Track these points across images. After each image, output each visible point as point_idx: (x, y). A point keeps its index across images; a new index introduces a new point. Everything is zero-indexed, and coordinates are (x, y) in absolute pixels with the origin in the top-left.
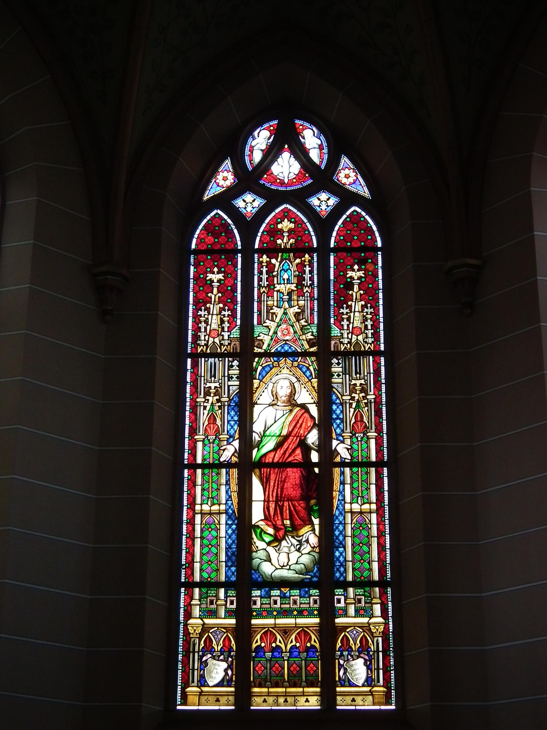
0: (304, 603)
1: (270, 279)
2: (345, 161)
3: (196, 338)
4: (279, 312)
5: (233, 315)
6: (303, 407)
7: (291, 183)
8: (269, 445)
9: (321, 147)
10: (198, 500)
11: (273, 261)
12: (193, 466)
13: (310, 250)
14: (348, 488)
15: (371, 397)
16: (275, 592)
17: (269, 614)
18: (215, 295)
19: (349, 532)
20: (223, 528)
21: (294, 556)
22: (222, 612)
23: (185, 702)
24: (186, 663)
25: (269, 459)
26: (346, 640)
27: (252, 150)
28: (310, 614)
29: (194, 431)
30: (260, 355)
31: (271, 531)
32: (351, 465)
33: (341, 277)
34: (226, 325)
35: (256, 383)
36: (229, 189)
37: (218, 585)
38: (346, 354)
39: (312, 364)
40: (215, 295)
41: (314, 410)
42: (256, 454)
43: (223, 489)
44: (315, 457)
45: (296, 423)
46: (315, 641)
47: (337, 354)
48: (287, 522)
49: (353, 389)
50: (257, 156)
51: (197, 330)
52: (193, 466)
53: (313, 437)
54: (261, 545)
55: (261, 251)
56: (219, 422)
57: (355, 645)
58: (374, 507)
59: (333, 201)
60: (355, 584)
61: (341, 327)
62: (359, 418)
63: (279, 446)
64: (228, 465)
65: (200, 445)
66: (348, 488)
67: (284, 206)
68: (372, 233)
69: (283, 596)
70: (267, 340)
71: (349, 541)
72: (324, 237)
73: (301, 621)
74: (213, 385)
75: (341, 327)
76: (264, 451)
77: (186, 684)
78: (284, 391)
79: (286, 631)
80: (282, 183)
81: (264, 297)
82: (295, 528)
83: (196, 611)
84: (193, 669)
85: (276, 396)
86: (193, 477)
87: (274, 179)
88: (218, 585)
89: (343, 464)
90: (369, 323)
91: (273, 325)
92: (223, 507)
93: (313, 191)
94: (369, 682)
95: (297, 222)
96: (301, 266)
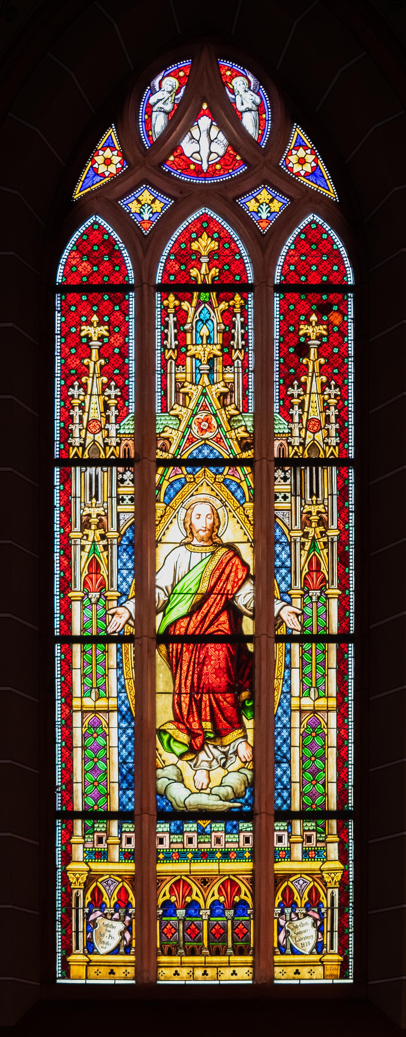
1: (180, 336)
3: (66, 433)
4: (195, 391)
5: (124, 397)
6: (231, 547)
7: (211, 172)
9: (260, 109)
10: (77, 690)
11: (185, 305)
14: (296, 674)
15: (333, 533)
16: (190, 827)
17: (182, 856)
19: (296, 739)
20: (114, 733)
21: (217, 774)
22: (115, 853)
23: (67, 975)
24: (66, 924)
25: (180, 630)
26: (288, 893)
27: (149, 109)
28: (240, 856)
29: (66, 585)
30: (165, 463)
31: (184, 738)
32: (302, 639)
34: (113, 412)
35: (160, 507)
36: (116, 180)
37: (108, 816)
43: (113, 674)
44: (248, 627)
46: (245, 895)
47: (282, 462)
48: (207, 725)
49: (306, 523)
54: (171, 758)
55: (165, 289)
56: (104, 571)
57: (301, 900)
58: (333, 702)
60: (303, 815)
61: (289, 418)
63: (196, 608)
64: (121, 639)
65: (76, 607)
66: (296, 674)
67: (203, 210)
68: (341, 263)
69: (202, 832)
70: (176, 436)
71: (296, 754)
73: (227, 866)
74: (94, 512)
75: (289, 418)
76: (172, 616)
77: (68, 951)
79: (205, 882)
80: (198, 171)
81: (171, 366)
82: (219, 734)
83: (78, 852)
84: (77, 932)
86: (68, 654)
88: (108, 816)
89: (289, 638)
90: (333, 412)
91: (185, 413)
92: (113, 703)
94: (319, 947)
95: (223, 239)
96: (228, 315)
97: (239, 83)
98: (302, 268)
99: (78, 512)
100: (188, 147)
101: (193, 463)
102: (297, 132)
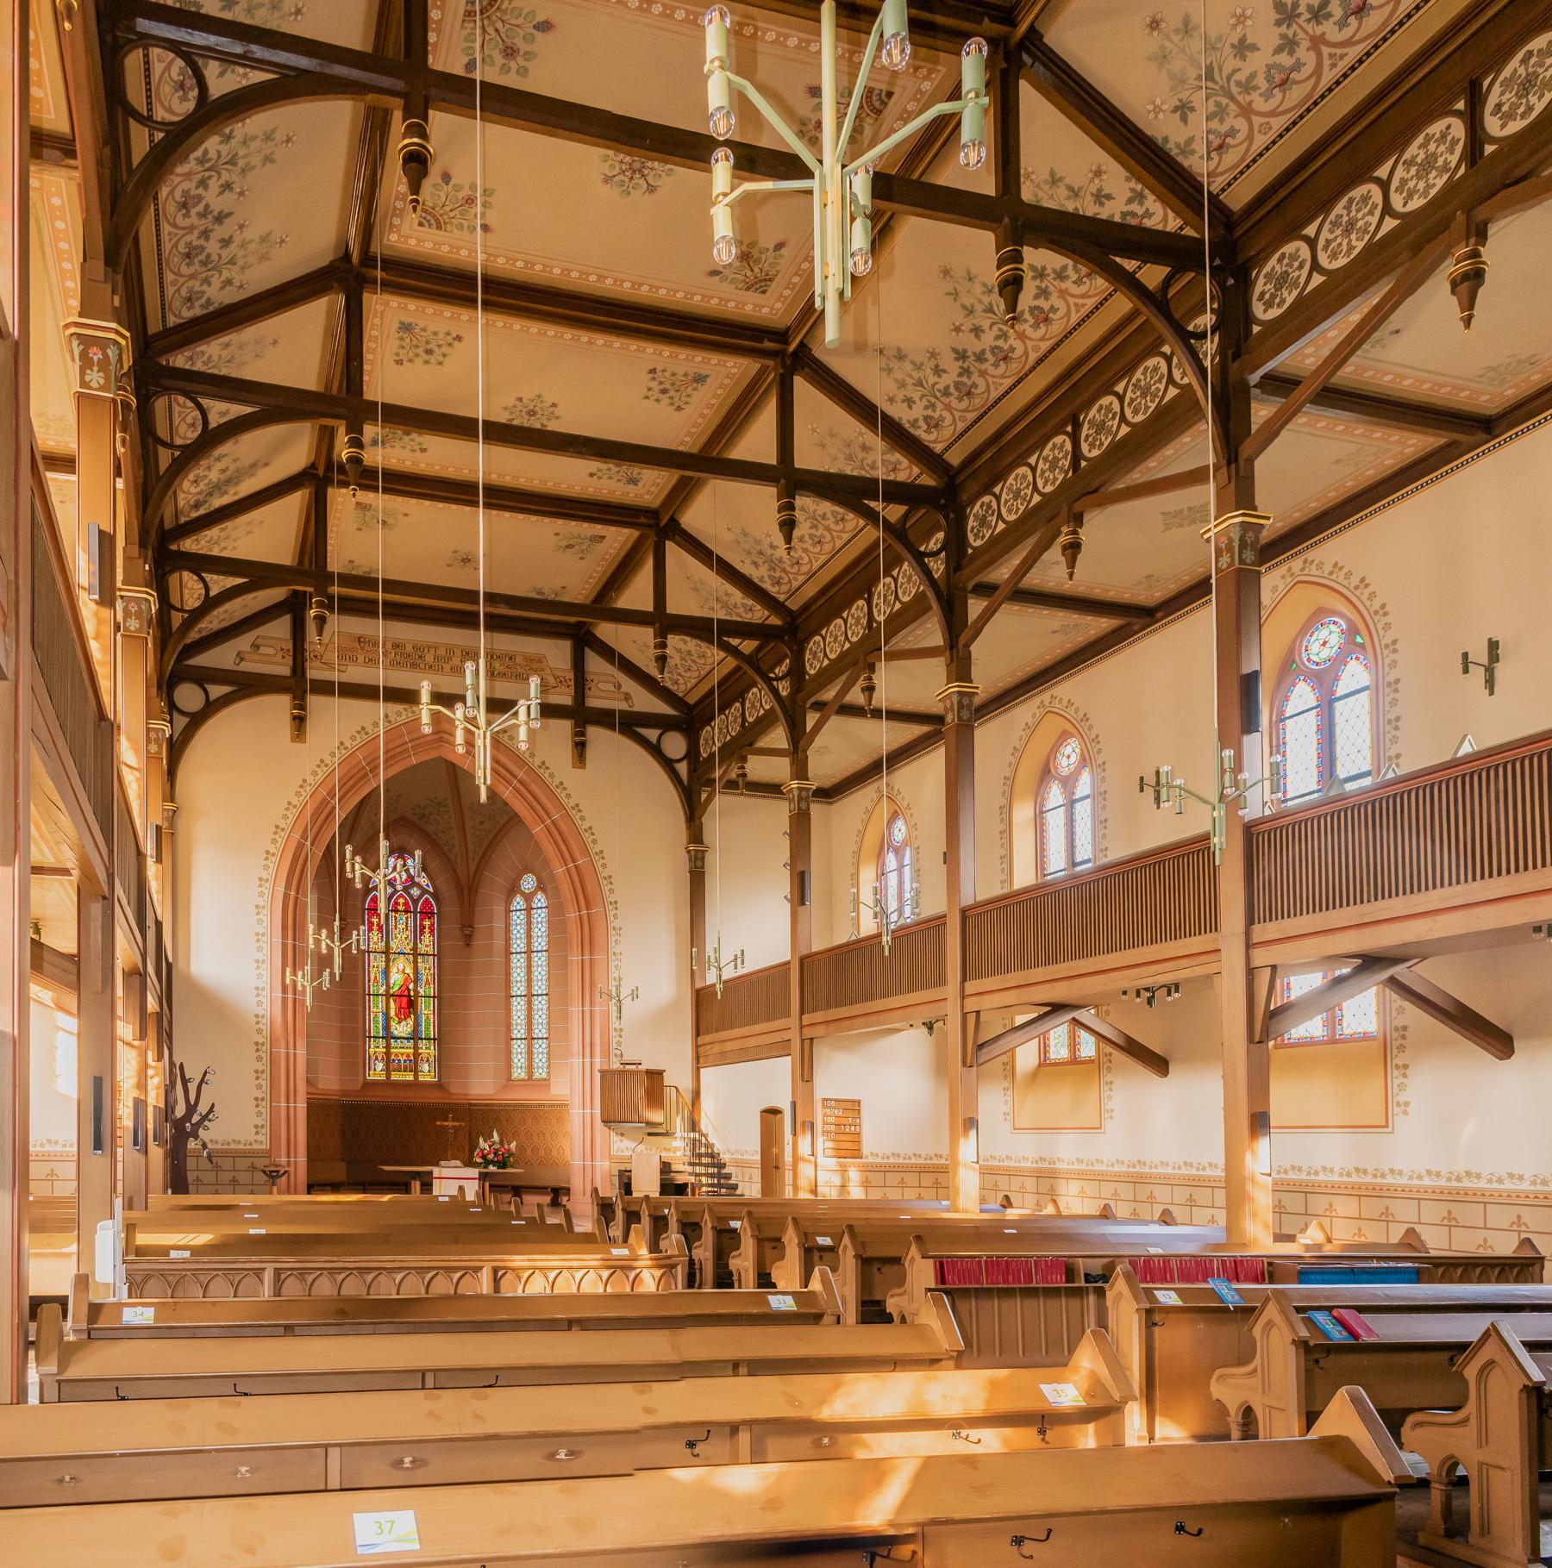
0: (408, 1045)
8: (396, 988)
33: (421, 925)
39: (411, 957)
42: (391, 991)
45: (406, 980)
78: (401, 968)
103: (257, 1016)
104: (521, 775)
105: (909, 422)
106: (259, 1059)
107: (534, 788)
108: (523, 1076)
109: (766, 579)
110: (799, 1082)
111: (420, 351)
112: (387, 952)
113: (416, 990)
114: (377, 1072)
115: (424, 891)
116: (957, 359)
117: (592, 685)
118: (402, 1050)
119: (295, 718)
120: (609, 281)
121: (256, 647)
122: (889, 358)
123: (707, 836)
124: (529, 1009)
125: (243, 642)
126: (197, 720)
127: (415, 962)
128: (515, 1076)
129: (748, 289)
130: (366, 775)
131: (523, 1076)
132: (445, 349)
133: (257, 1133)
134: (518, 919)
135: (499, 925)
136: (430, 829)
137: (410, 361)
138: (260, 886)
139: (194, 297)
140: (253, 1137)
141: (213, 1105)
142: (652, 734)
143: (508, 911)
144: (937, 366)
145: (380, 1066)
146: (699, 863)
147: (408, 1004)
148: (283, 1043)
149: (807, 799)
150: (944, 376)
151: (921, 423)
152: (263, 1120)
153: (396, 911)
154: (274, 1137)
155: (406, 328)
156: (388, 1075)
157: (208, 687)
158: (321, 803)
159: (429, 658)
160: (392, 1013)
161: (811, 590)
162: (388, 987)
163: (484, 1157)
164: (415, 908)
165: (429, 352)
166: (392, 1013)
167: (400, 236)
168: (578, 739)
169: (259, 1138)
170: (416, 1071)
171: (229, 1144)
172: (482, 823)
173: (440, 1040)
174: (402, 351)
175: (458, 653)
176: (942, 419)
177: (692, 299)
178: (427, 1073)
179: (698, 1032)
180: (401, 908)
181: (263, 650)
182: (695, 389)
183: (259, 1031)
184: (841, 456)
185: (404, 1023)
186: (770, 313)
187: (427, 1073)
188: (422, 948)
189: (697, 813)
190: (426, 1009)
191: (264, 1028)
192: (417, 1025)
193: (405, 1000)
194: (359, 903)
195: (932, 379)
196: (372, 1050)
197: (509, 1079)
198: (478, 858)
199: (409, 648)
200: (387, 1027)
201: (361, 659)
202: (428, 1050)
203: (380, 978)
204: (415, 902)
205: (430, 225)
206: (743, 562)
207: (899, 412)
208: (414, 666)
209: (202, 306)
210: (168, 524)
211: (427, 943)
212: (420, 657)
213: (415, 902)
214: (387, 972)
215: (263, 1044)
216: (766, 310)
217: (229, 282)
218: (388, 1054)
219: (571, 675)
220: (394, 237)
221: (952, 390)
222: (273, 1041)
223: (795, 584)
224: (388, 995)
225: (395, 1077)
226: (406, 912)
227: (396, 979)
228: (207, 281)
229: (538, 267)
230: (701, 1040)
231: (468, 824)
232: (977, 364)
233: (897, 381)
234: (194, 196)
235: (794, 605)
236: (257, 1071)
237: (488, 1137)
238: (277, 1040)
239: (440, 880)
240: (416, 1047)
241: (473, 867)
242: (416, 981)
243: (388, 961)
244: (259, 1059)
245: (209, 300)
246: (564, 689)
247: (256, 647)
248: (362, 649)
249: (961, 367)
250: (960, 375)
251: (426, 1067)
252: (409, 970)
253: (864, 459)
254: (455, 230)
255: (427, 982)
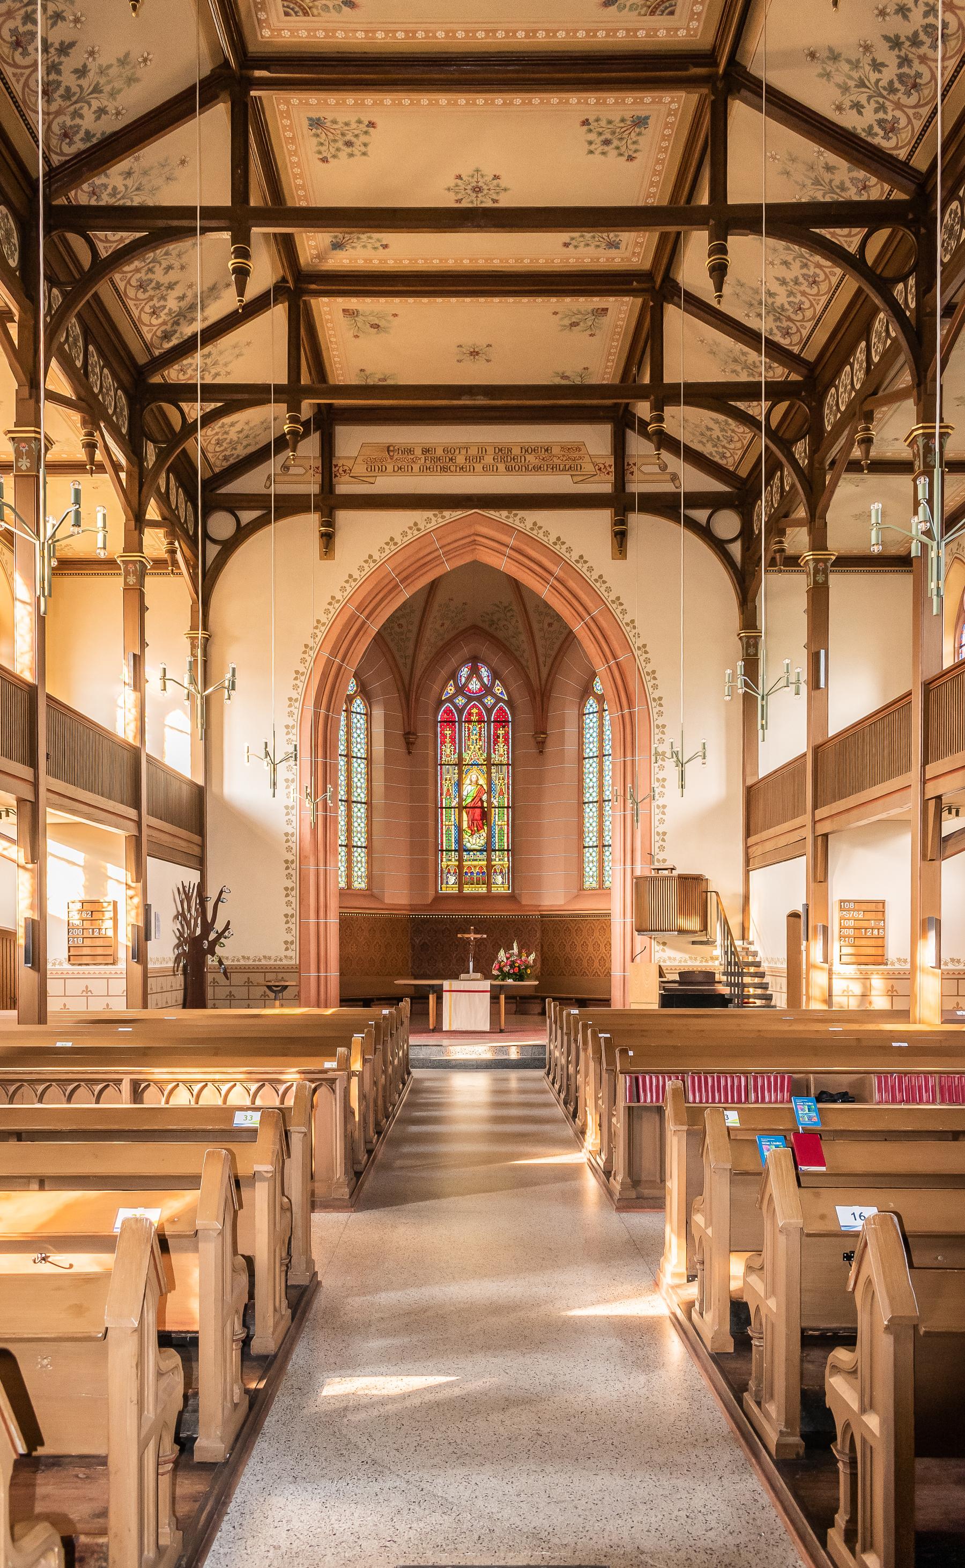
0: (481, 857)
2: (497, 682)
8: (469, 800)
12: (442, 808)
13: (484, 722)
18: (448, 740)
29: (441, 794)
33: (495, 734)
36: (453, 695)
38: (497, 765)
40: (448, 740)
41: (485, 787)
42: (464, 804)
44: (485, 804)
45: (479, 792)
46: (485, 870)
47: (493, 765)
50: (463, 680)
51: (441, 754)
52: (442, 808)
53: (485, 797)
55: (465, 722)
57: (498, 871)
59: (492, 701)
62: (501, 790)
68: (506, 714)
72: (489, 716)
73: (481, 863)
78: (474, 780)
79: (475, 867)
85: (471, 781)
87: (469, 690)
93: (485, 696)
94: (503, 883)
95: (479, 709)
96: (480, 728)
97: (483, 670)
98: (499, 717)
99: (444, 777)
100: (470, 686)
101: (472, 765)
102: (497, 682)
103: (286, 834)
104: (557, 571)
105: (864, 130)
106: (289, 876)
107: (571, 584)
108: (594, 885)
109: (775, 331)
110: (812, 885)
111: (340, 144)
112: (460, 764)
113: (489, 801)
114: (450, 885)
115: (499, 700)
116: (892, 48)
117: (635, 469)
118: (475, 863)
119: (323, 535)
120: (500, 34)
121: (286, 468)
122: (823, 62)
123: (762, 622)
124: (601, 815)
125: (272, 465)
126: (229, 547)
127: (489, 773)
128: (587, 885)
129: (653, 13)
130: (397, 586)
131: (594, 885)
132: (363, 138)
133: (287, 949)
134: (591, 722)
135: (570, 730)
136: (500, 635)
137: (334, 156)
138: (290, 706)
139: (70, 132)
140: (283, 954)
141: (229, 922)
142: (701, 515)
143: (582, 715)
144: (874, 60)
145: (452, 879)
146: (751, 651)
147: (482, 815)
148: (312, 860)
149: (825, 572)
150: (884, 70)
151: (877, 129)
152: (293, 936)
153: (470, 722)
154: (303, 953)
155: (316, 123)
156: (461, 888)
157: (238, 513)
158: (350, 620)
159: (460, 459)
160: (465, 825)
161: (821, 337)
162: (461, 799)
163: (500, 969)
164: (489, 717)
165: (349, 144)
166: (465, 825)
167: (272, 30)
168: (617, 528)
169: (289, 953)
170: (489, 884)
171: (260, 960)
172: (550, 625)
173: (513, 851)
174: (323, 149)
175: (490, 451)
176: (896, 120)
177: (595, 36)
178: (500, 885)
179: (748, 833)
180: (474, 718)
181: (293, 471)
182: (639, 134)
183: (289, 849)
184: (809, 182)
185: (477, 835)
186: (688, 34)
187: (500, 885)
188: (496, 758)
189: (750, 597)
190: (500, 820)
191: (293, 846)
192: (490, 836)
193: (478, 811)
194: (430, 717)
195: (874, 76)
196: (444, 864)
197: (581, 889)
198: (550, 661)
199: (439, 452)
200: (459, 840)
201: (390, 468)
202: (501, 861)
203: (453, 791)
204: (489, 711)
205: (296, 13)
206: (747, 315)
207: (849, 120)
208: (444, 469)
209: (82, 140)
210: (142, 359)
211: (501, 753)
212: (451, 459)
213: (489, 711)
214: (459, 784)
215: (292, 862)
216: (681, 33)
217: (102, 111)
218: (460, 867)
219: (611, 461)
220: (266, 33)
221: (897, 85)
222: (302, 858)
223: (805, 333)
224: (460, 808)
225: (467, 890)
226: (480, 722)
227: (469, 790)
228: (77, 114)
229: (420, 35)
230: (751, 840)
231: (536, 626)
232: (913, 50)
233: (839, 86)
234: (25, 34)
235: (810, 355)
236: (287, 889)
237: (509, 947)
238: (306, 857)
239: (513, 687)
240: (489, 860)
241: (544, 671)
242: (489, 792)
243: (460, 773)
244: (289, 876)
245: (87, 133)
246: (604, 477)
247: (286, 468)
248: (391, 458)
249: (899, 57)
250: (900, 66)
251: (499, 879)
252: (482, 781)
253: (831, 181)
254: (323, 13)
255: (501, 793)
